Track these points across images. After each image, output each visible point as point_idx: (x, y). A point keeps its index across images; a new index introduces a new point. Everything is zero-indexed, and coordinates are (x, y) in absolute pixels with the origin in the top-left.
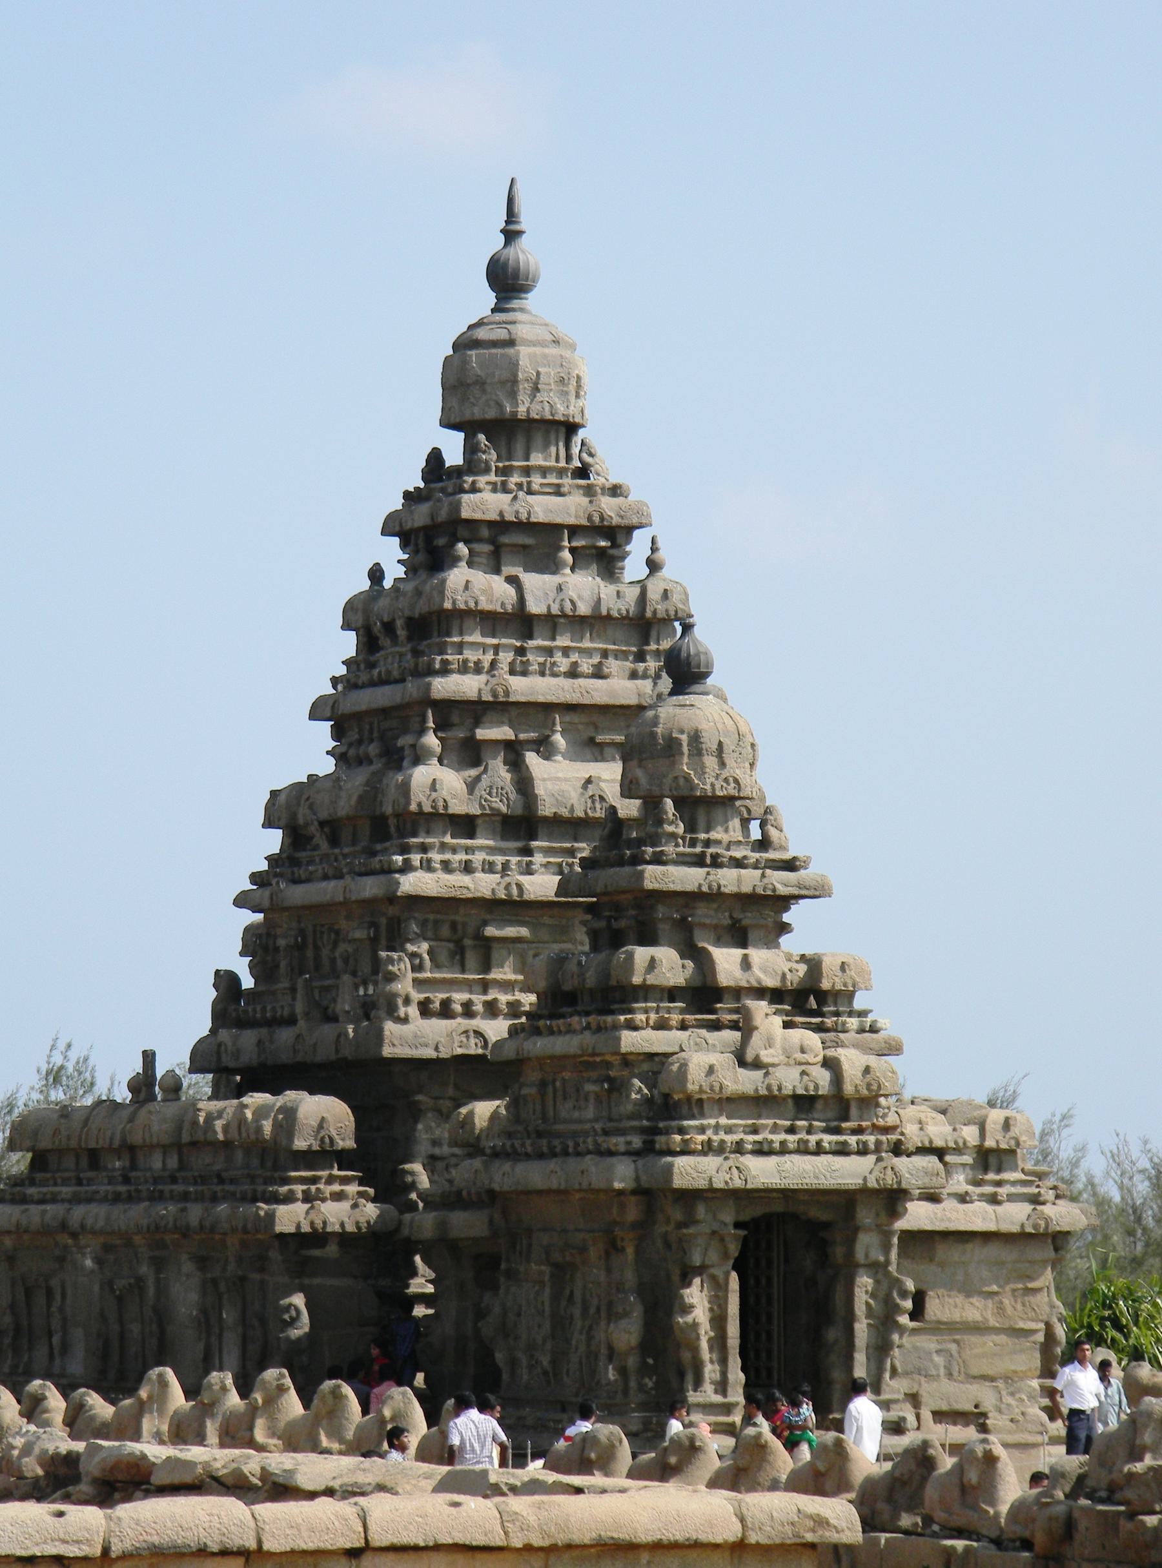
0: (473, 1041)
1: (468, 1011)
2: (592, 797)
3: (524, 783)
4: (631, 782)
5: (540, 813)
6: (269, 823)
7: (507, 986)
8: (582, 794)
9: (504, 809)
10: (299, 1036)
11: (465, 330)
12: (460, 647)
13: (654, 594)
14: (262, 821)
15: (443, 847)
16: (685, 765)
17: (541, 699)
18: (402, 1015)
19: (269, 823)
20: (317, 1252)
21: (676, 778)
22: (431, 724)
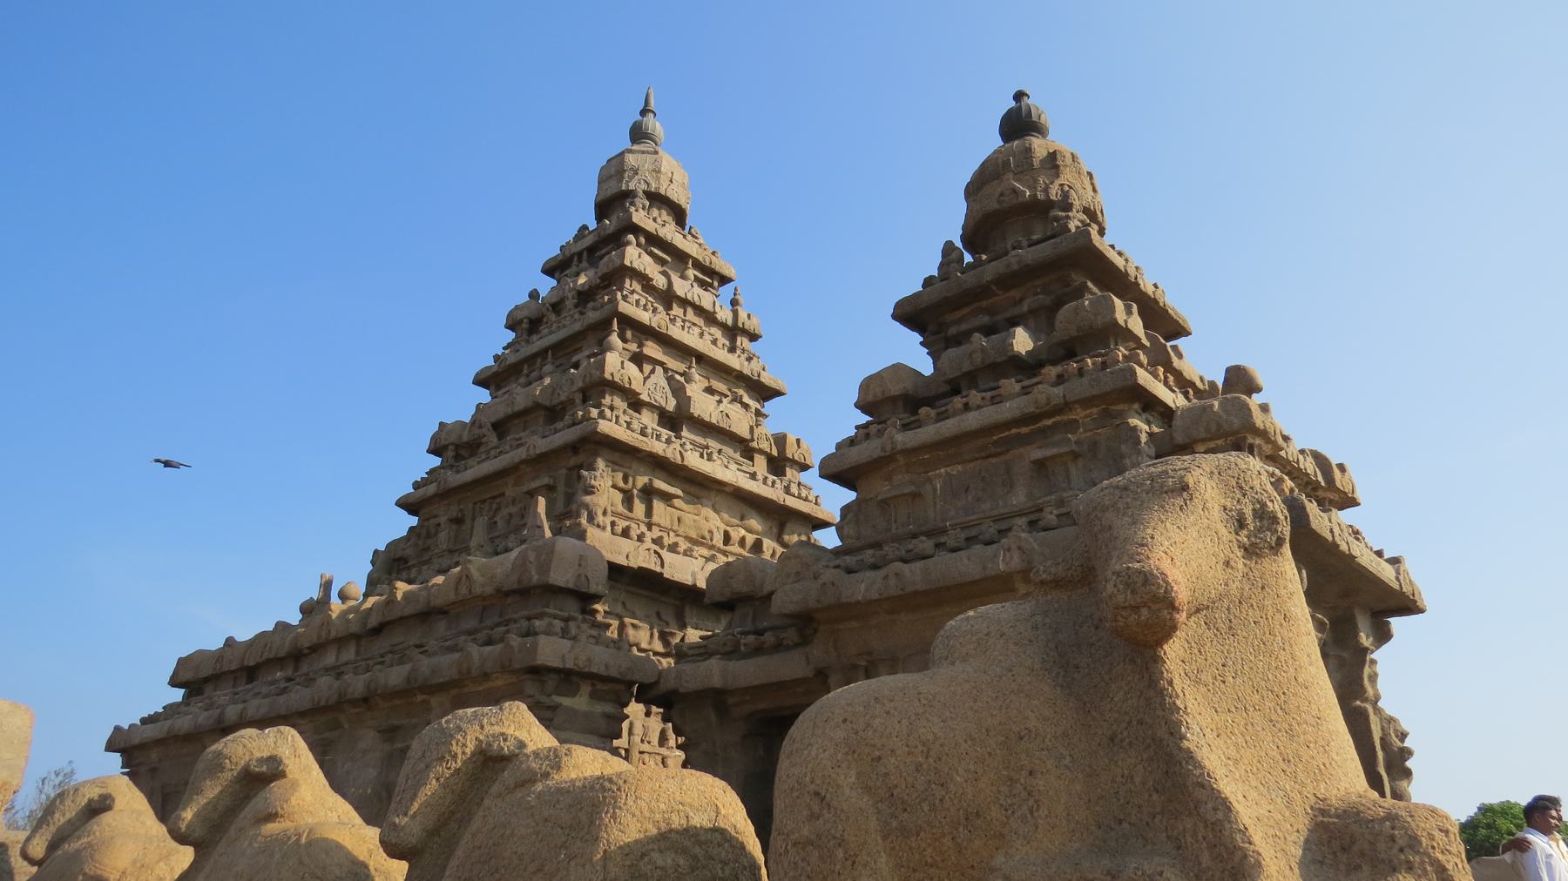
0: (654, 558)
3: (678, 391)
4: (1002, 195)
5: (692, 411)
6: (435, 450)
7: (668, 531)
8: (716, 408)
9: (664, 405)
12: (633, 292)
13: (743, 315)
16: (1067, 177)
17: (685, 342)
18: (601, 524)
19: (435, 450)
20: (566, 701)
21: (1062, 185)
22: (615, 327)
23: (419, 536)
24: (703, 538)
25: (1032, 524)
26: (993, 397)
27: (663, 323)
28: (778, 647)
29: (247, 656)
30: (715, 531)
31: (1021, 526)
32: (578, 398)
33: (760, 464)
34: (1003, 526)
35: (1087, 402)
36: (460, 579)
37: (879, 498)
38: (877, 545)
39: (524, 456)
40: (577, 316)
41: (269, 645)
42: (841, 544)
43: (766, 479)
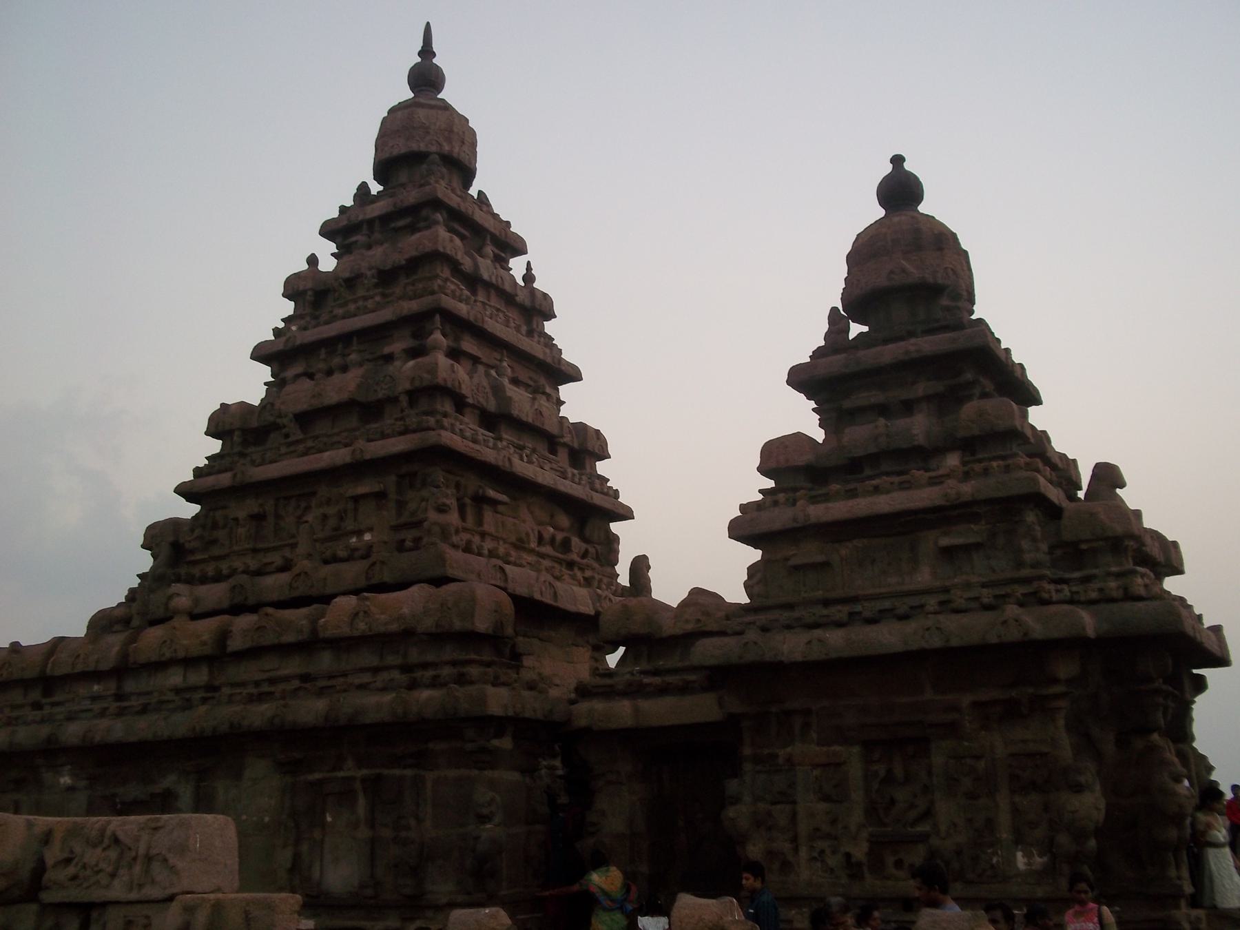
0: (499, 575)
1: (480, 554)
2: (536, 409)
3: (497, 390)
4: (892, 272)
8: (531, 407)
9: (485, 404)
10: (299, 575)
11: (397, 103)
12: (446, 280)
13: (539, 296)
14: (205, 430)
15: (456, 419)
18: (455, 543)
20: (496, 742)
21: (946, 268)
23: (203, 527)
24: (520, 540)
25: (941, 603)
26: (901, 483)
27: (479, 316)
28: (684, 689)
29: (50, 665)
30: (530, 532)
31: (932, 606)
32: (404, 400)
33: (563, 457)
34: (915, 601)
35: (990, 502)
36: (357, 614)
37: (792, 562)
38: (790, 606)
39: (348, 459)
40: (378, 298)
41: (82, 657)
42: (748, 601)
43: (574, 475)
